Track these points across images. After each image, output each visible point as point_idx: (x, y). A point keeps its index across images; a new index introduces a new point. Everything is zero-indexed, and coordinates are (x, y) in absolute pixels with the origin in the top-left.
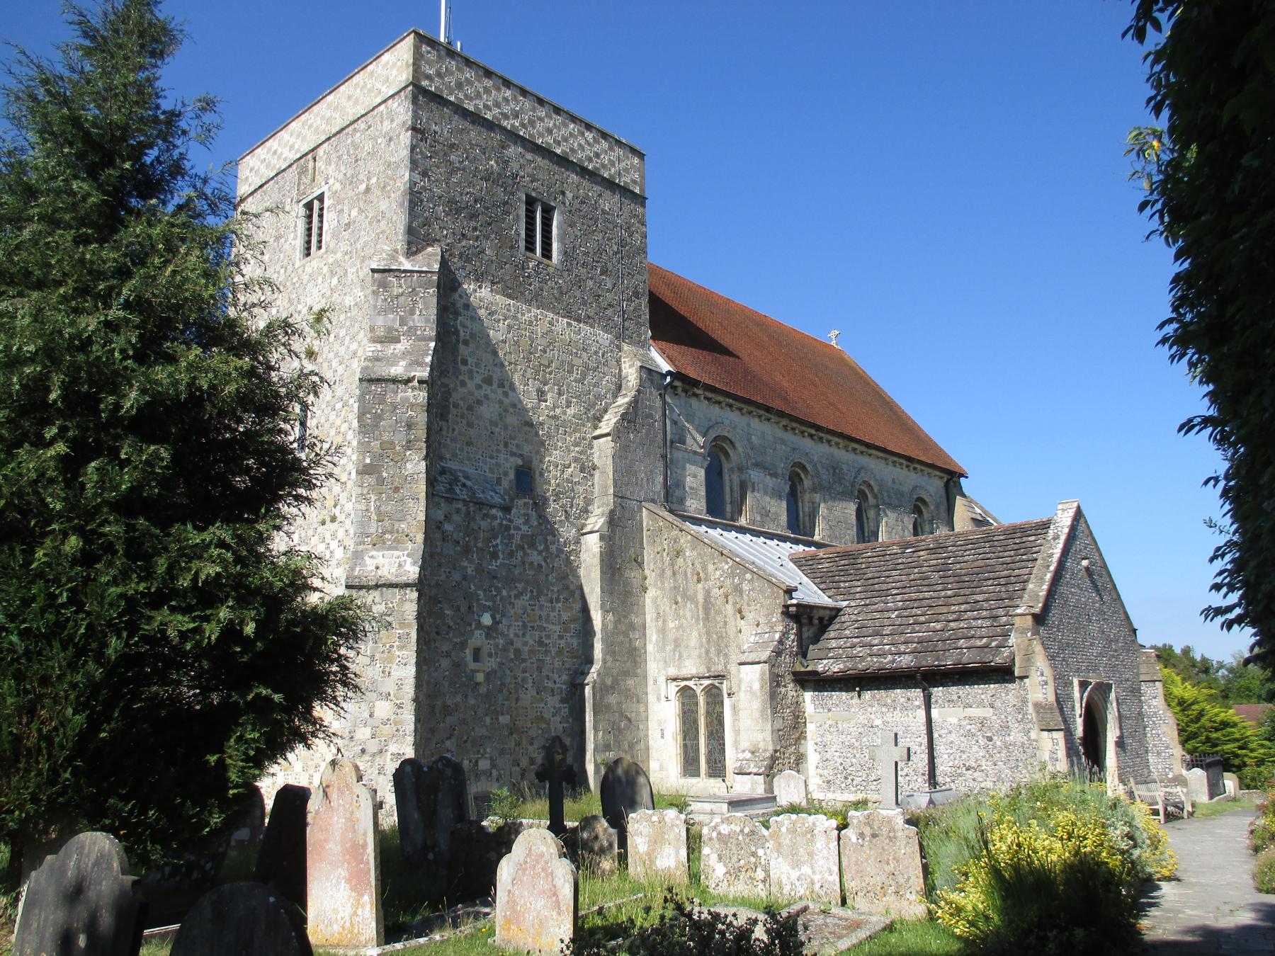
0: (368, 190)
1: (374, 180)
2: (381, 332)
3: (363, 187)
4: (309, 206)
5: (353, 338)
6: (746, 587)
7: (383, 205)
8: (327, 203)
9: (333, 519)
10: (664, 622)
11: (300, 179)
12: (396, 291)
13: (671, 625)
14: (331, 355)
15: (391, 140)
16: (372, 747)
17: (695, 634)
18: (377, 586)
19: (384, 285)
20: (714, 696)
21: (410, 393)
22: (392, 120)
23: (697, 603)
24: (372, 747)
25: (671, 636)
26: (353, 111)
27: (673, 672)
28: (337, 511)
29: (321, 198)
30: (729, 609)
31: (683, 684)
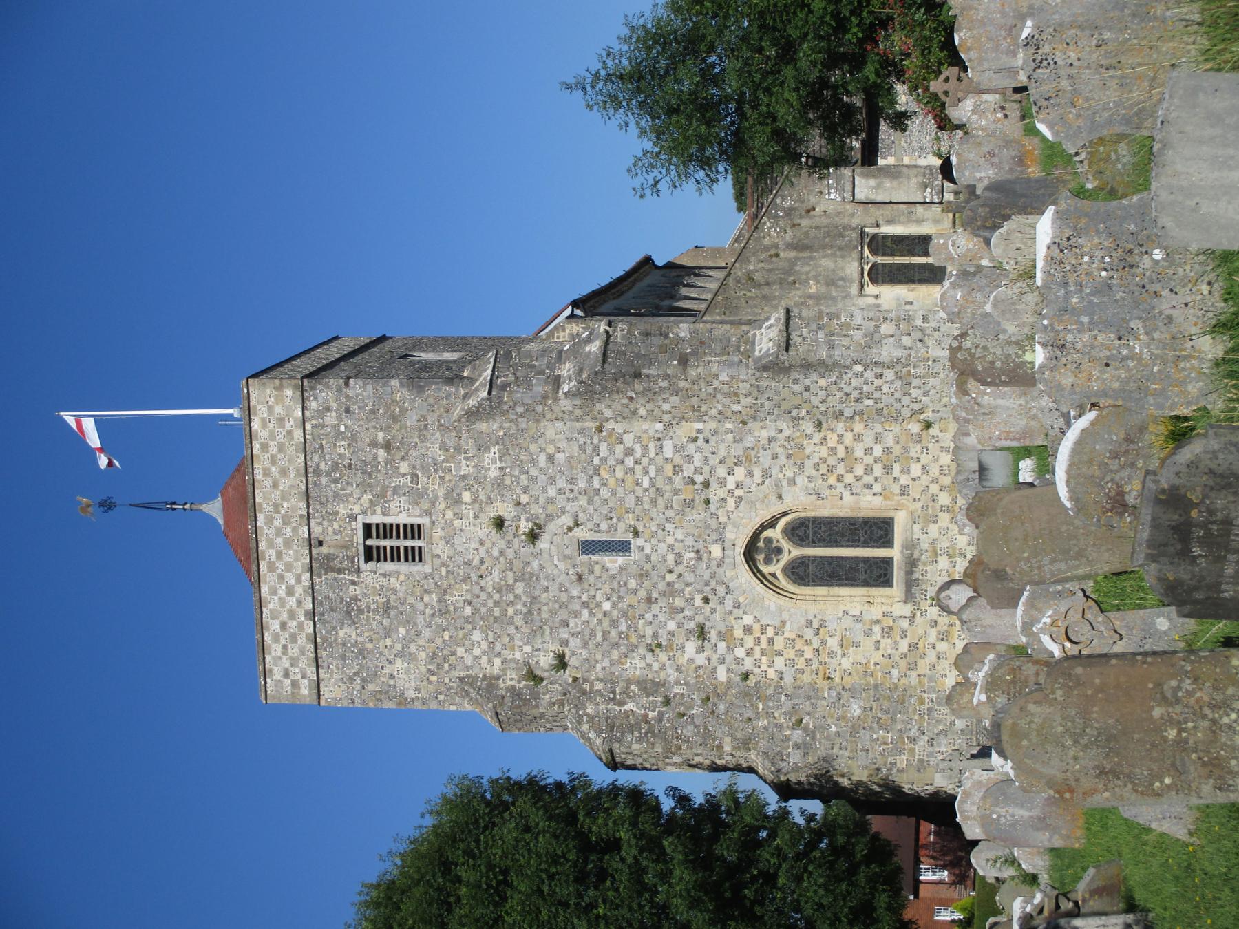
0: (387, 446)
1: (381, 435)
2: (548, 388)
3: (382, 453)
4: (370, 554)
5: (533, 461)
6: (788, 204)
7: (411, 420)
8: (376, 519)
9: (706, 485)
10: (810, 297)
11: (333, 570)
12: (511, 378)
13: (813, 290)
14: (542, 500)
15: (348, 411)
16: (919, 335)
17: (824, 262)
18: (788, 335)
19: (503, 387)
20: (879, 244)
21: (619, 334)
22: (328, 409)
23: (797, 259)
24: (919, 335)
25: (823, 289)
26: (293, 482)
27: (854, 289)
28: (699, 479)
29: (367, 528)
30: (804, 223)
31: (866, 277)
